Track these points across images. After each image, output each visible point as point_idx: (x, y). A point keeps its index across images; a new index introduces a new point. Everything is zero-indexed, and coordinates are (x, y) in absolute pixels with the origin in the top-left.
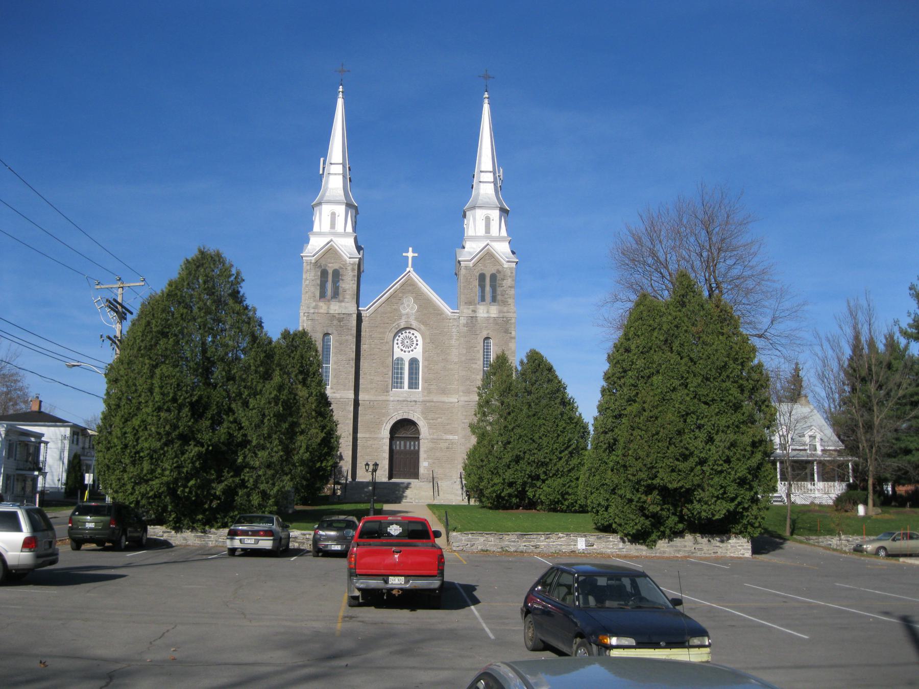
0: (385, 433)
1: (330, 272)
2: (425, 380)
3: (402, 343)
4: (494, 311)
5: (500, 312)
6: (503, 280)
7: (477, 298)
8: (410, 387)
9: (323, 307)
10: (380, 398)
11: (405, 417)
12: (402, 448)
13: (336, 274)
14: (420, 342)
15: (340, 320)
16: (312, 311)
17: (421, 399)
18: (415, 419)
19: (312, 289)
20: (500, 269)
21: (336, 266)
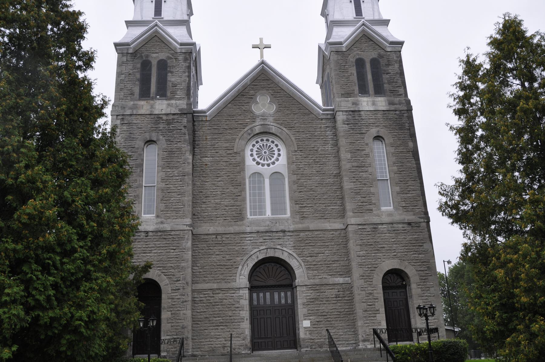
0: (242, 279)
1: (154, 63)
2: (295, 201)
3: (259, 154)
4: (381, 103)
5: (391, 103)
6: (388, 65)
7: (356, 88)
8: (273, 212)
9: (144, 107)
10: (232, 229)
11: (271, 254)
12: (268, 302)
13: (163, 66)
14: (283, 152)
15: (169, 123)
16: (128, 112)
17: (292, 228)
18: (284, 257)
19: (129, 86)
20: (382, 52)
21: (163, 56)
